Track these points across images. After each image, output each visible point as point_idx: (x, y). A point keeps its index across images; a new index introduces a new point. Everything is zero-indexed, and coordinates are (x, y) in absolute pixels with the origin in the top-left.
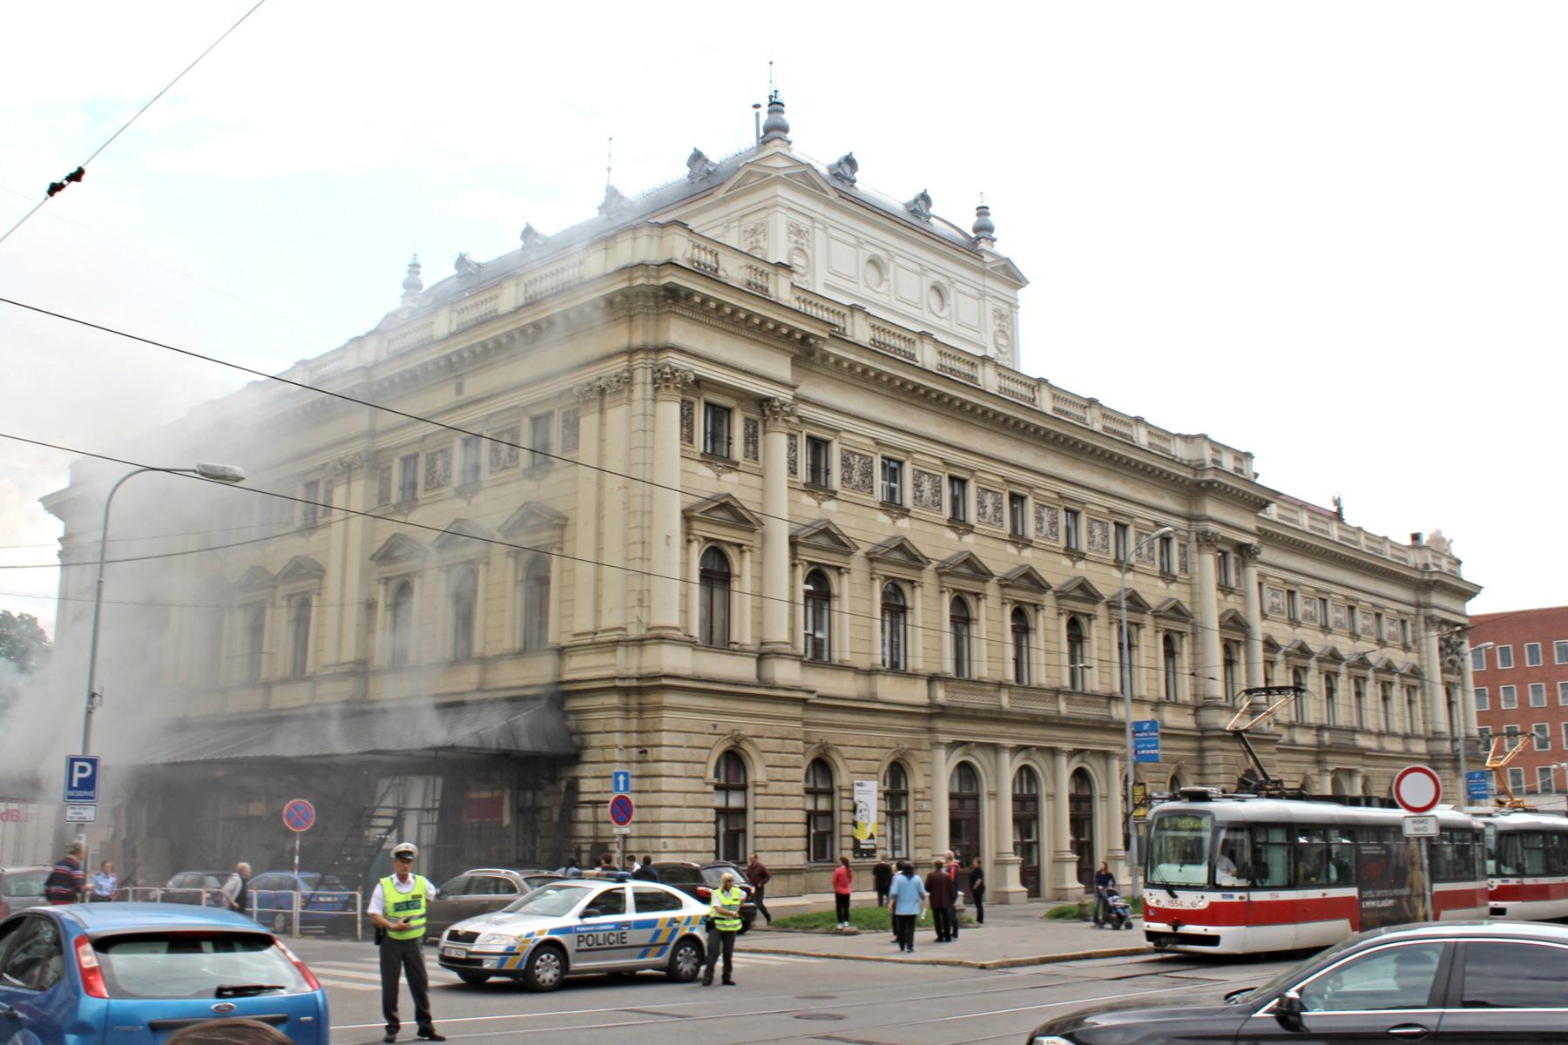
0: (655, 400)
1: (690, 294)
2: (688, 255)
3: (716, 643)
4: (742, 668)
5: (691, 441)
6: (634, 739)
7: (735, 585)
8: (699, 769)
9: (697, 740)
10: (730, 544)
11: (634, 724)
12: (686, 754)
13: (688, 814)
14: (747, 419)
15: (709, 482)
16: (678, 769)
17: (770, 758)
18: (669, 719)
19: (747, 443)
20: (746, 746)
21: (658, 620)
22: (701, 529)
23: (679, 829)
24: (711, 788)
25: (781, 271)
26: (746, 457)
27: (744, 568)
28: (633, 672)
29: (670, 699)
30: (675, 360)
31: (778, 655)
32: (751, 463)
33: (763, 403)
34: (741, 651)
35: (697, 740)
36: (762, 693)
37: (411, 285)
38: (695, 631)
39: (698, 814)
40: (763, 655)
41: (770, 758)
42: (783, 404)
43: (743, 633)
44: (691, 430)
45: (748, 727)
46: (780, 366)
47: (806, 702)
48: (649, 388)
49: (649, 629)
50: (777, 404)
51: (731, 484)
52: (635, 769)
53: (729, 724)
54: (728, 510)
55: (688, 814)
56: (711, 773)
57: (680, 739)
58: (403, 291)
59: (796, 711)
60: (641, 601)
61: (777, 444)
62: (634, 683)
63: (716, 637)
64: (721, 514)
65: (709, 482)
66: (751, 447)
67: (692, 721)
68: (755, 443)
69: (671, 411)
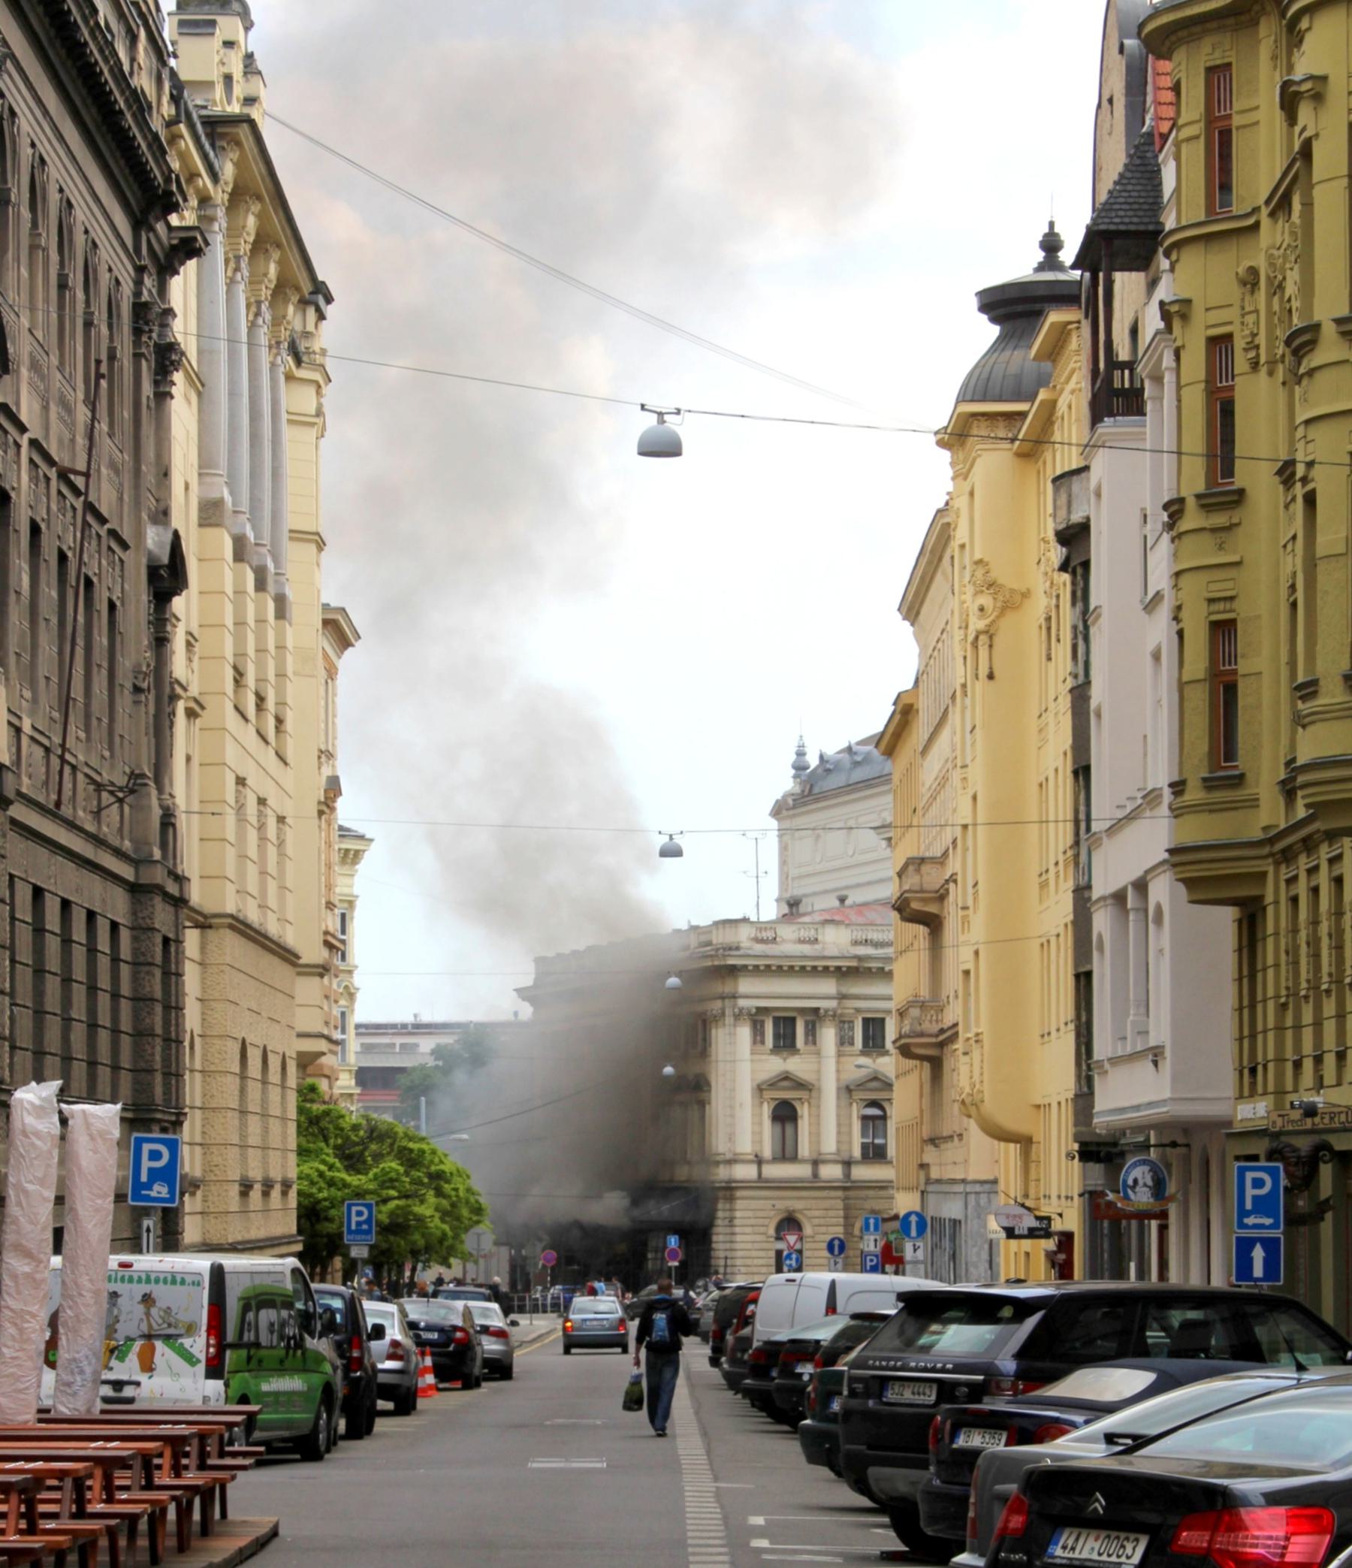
0: (735, 1026)
1: (745, 967)
2: (753, 935)
3: (787, 1155)
4: (799, 1171)
5: (763, 1042)
6: (727, 1214)
7: (800, 1122)
8: (762, 1229)
9: (759, 1214)
10: (794, 1099)
11: (728, 1206)
12: (753, 1221)
13: (754, 1254)
14: (807, 1023)
15: (775, 1065)
16: (748, 1230)
17: (816, 1221)
18: (739, 1204)
19: (807, 1035)
20: (799, 1216)
21: (739, 1150)
22: (768, 1095)
23: (749, 1262)
24: (773, 1239)
25: (826, 926)
26: (806, 1043)
27: (804, 1111)
28: (726, 1178)
29: (739, 1193)
30: (742, 1003)
31: (825, 1162)
32: (811, 1048)
33: (816, 1010)
34: (804, 1161)
35: (759, 1214)
36: (814, 1184)
37: (799, 767)
38: (767, 1153)
39: (762, 1254)
40: (816, 1163)
41: (816, 1221)
42: (826, 1011)
43: (804, 1150)
44: (763, 1034)
45: (797, 1205)
46: (828, 987)
47: (848, 1187)
48: (732, 1019)
49: (735, 1154)
50: (822, 1011)
51: (796, 1065)
52: (728, 1230)
53: (781, 1205)
54: (786, 1078)
55: (754, 1254)
56: (772, 1231)
57: (750, 1214)
58: (793, 772)
59: (840, 1193)
60: (730, 1139)
61: (828, 1035)
62: (723, 1185)
63: (786, 1153)
64: (785, 1084)
65: (775, 1065)
66: (810, 1038)
67: (754, 1204)
68: (814, 1035)
69: (745, 1032)
